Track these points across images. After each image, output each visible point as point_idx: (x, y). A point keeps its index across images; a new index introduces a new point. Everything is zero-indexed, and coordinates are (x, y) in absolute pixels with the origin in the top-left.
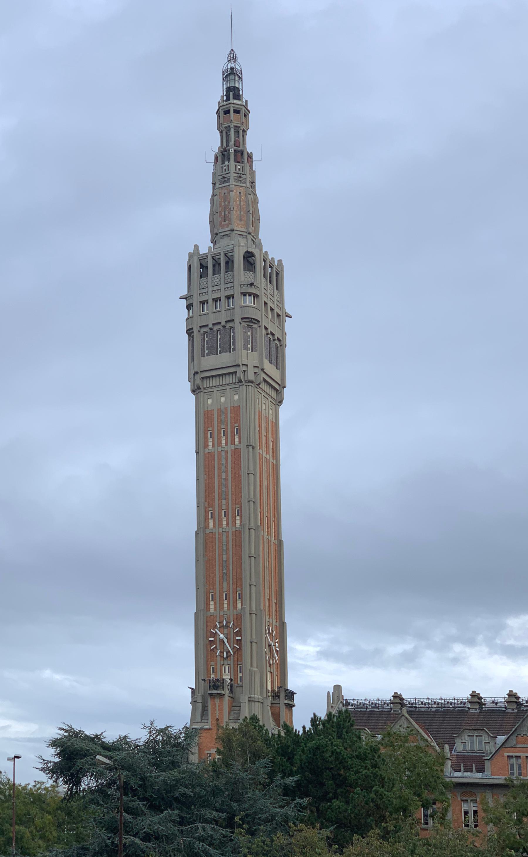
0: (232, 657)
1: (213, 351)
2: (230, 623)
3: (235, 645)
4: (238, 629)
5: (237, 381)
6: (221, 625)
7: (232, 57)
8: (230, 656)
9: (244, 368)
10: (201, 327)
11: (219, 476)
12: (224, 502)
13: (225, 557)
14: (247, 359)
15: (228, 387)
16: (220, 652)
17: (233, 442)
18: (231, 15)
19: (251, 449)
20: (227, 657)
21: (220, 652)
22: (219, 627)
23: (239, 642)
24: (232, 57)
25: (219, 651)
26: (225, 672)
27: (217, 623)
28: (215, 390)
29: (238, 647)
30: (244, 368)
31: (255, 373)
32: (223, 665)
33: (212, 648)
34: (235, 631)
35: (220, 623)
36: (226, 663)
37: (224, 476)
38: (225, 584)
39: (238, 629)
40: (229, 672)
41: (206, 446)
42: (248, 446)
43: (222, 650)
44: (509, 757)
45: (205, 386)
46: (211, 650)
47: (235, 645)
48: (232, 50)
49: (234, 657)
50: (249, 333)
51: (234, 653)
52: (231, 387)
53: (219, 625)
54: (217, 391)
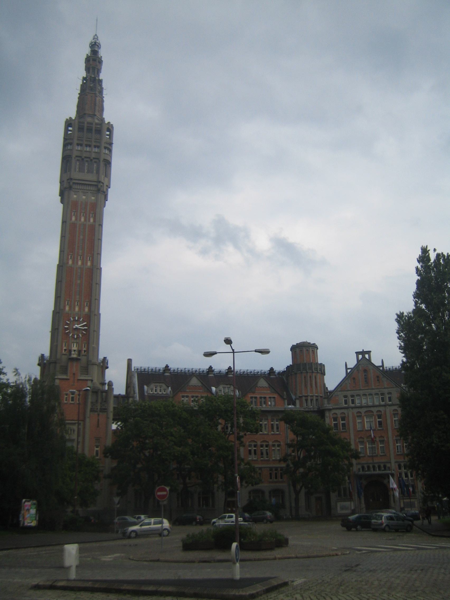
0: (80, 339)
1: (81, 170)
2: (81, 319)
5: (96, 190)
6: (74, 319)
7: (96, 37)
9: (102, 185)
11: (79, 237)
12: (81, 251)
13: (79, 282)
14: (104, 180)
17: (89, 220)
18: (97, 20)
20: (77, 338)
21: (72, 335)
24: (96, 37)
26: (74, 346)
28: (80, 191)
30: (102, 185)
31: (106, 189)
35: (73, 318)
36: (75, 341)
37: (81, 237)
38: (78, 297)
40: (76, 346)
41: (71, 219)
44: (252, 398)
48: (96, 35)
51: (82, 336)
52: (91, 192)
53: (73, 319)
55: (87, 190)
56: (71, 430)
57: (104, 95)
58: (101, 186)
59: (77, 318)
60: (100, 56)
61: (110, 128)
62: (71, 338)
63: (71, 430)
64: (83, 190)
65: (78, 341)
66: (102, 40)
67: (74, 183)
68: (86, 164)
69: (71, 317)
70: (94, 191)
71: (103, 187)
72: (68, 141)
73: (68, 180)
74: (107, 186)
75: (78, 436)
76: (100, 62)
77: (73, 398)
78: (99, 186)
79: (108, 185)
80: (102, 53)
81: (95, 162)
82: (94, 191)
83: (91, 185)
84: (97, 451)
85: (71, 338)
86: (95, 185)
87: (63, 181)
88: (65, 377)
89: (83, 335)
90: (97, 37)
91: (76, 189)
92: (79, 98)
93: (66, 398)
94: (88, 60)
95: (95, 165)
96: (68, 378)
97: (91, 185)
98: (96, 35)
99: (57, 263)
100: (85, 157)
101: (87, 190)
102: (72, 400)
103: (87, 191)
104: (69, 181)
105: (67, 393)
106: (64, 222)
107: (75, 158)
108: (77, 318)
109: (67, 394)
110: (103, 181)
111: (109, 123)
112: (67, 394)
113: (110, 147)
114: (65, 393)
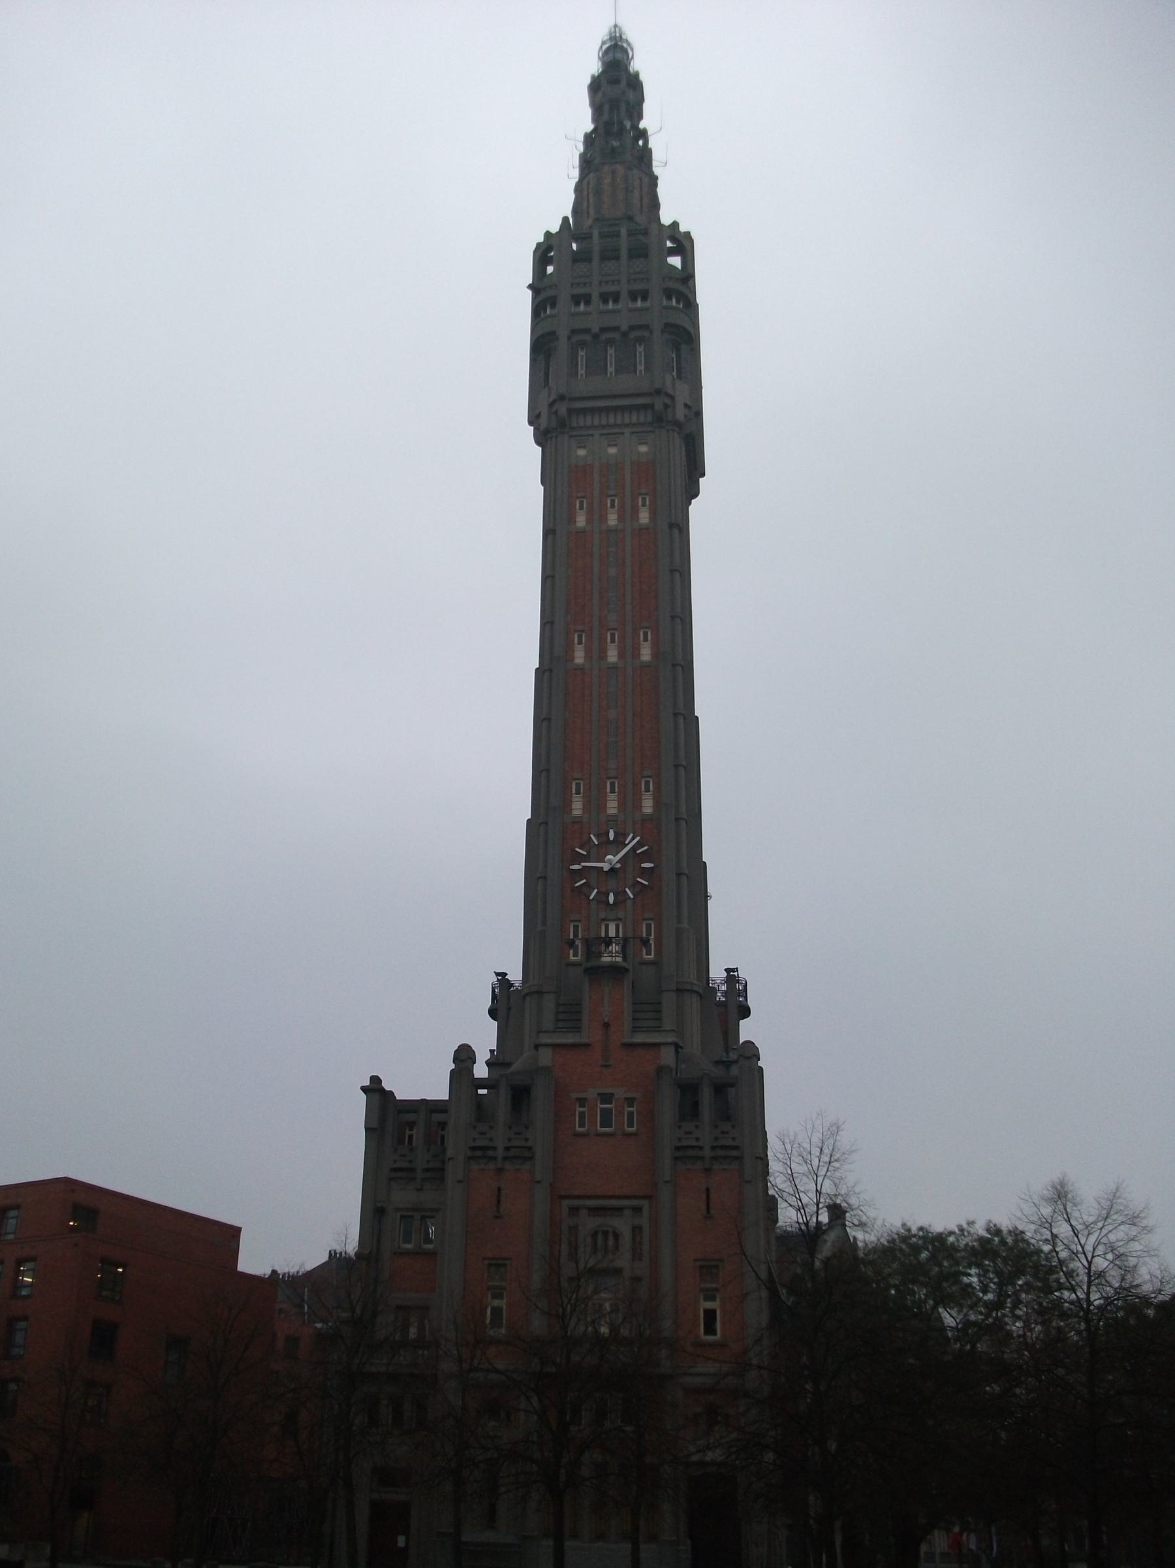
0: (629, 903)
3: (639, 880)
4: (646, 848)
5: (650, 419)
6: (604, 839)
8: (624, 901)
9: (667, 401)
10: (574, 332)
15: (627, 431)
16: (597, 892)
19: (676, 531)
22: (597, 843)
23: (644, 873)
25: (596, 891)
27: (592, 836)
29: (646, 883)
30: (667, 401)
32: (603, 920)
33: (577, 885)
34: (638, 852)
35: (597, 836)
39: (646, 848)
41: (572, 520)
42: (671, 526)
43: (604, 890)
45: (575, 424)
46: (573, 889)
47: (639, 880)
49: (634, 903)
50: (674, 355)
54: (601, 435)
55: (616, 425)
56: (605, 1233)
57: (657, 170)
58: (666, 406)
59: (611, 836)
60: (631, 69)
61: (683, 244)
62: (594, 905)
63: (605, 1233)
64: (603, 427)
65: (621, 914)
66: (632, 35)
67: (570, 411)
68: (611, 351)
69: (590, 834)
70: (642, 424)
71: (674, 408)
72: (544, 295)
73: (551, 405)
74: (686, 406)
75: (636, 1254)
76: (635, 84)
77: (606, 1114)
78: (659, 406)
79: (689, 404)
80: (640, 64)
81: (640, 340)
82: (642, 424)
83: (630, 408)
84: (710, 1315)
85: (594, 905)
86: (645, 407)
87: (539, 416)
88: (570, 1039)
89: (640, 890)
90: (620, 30)
91: (581, 428)
92: (579, 189)
93: (582, 1115)
94: (596, 86)
95: (640, 349)
96: (585, 1040)
97: (630, 408)
98: (616, 26)
99: (536, 664)
100: (603, 330)
101: (616, 425)
102: (606, 1122)
103: (617, 430)
104: (555, 408)
105: (580, 1095)
106: (549, 533)
107: (569, 338)
108: (611, 836)
109: (582, 1102)
110: (670, 391)
111: (675, 225)
112: (582, 1102)
113: (683, 289)
114: (575, 1096)
